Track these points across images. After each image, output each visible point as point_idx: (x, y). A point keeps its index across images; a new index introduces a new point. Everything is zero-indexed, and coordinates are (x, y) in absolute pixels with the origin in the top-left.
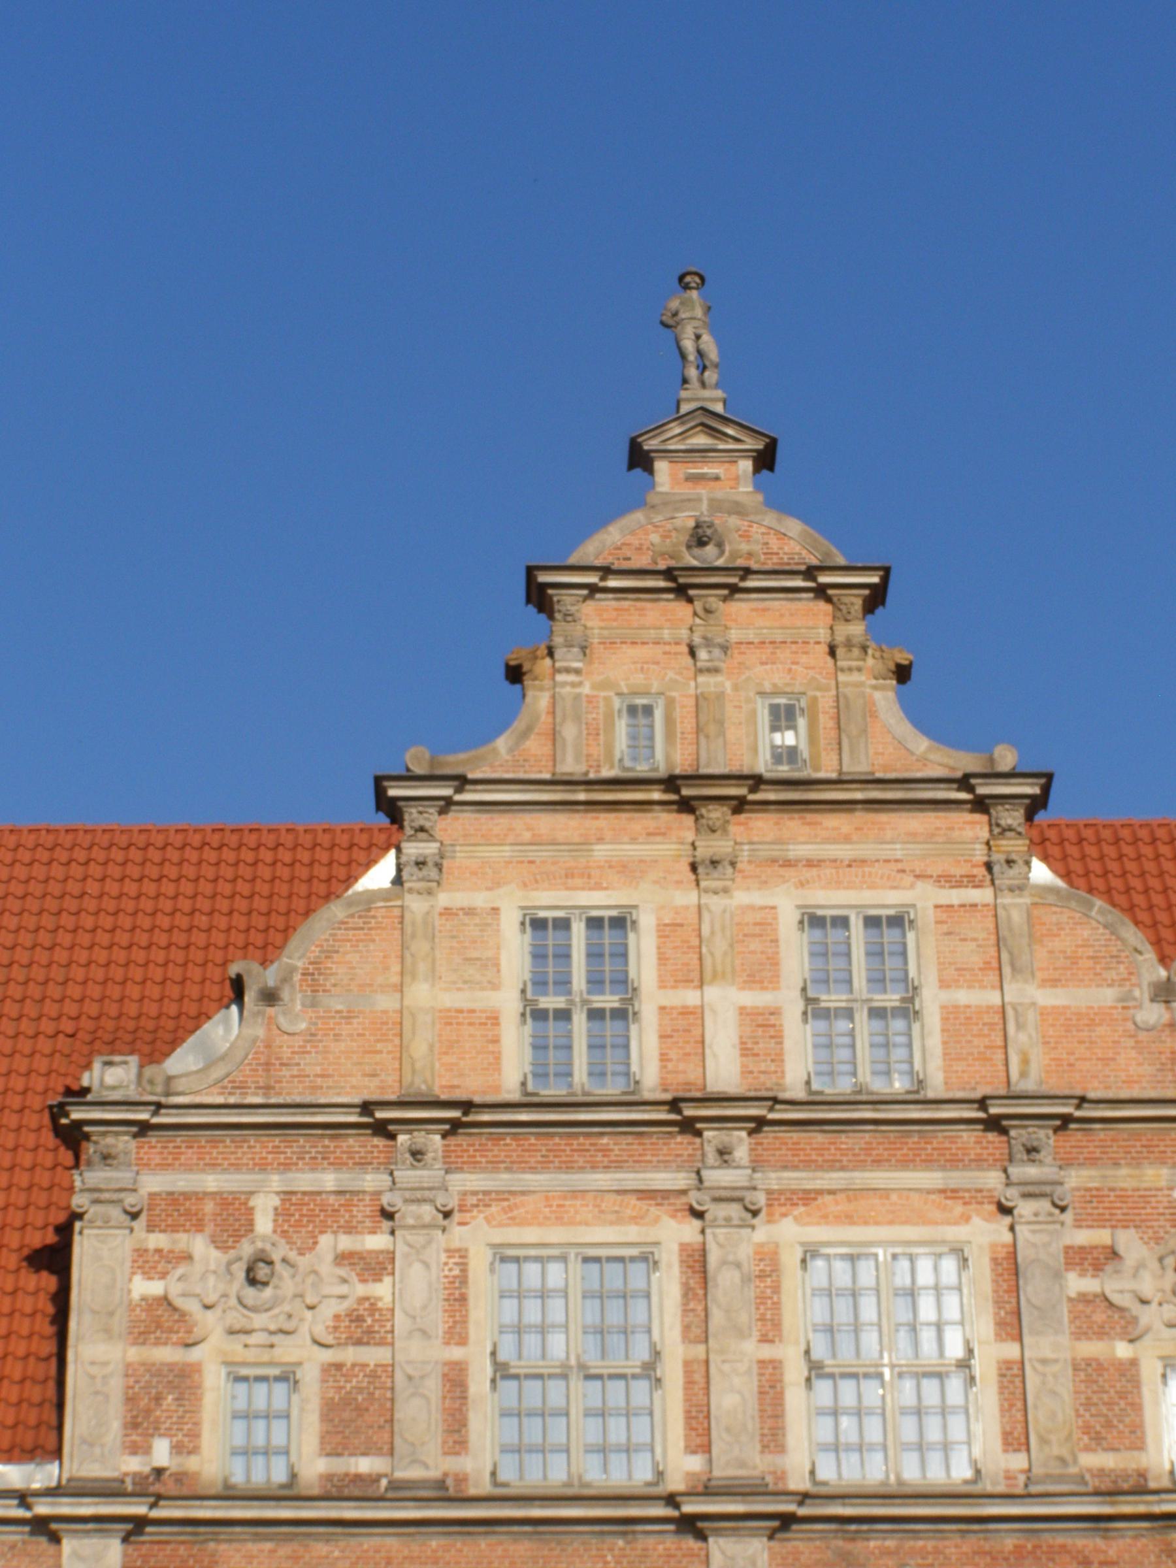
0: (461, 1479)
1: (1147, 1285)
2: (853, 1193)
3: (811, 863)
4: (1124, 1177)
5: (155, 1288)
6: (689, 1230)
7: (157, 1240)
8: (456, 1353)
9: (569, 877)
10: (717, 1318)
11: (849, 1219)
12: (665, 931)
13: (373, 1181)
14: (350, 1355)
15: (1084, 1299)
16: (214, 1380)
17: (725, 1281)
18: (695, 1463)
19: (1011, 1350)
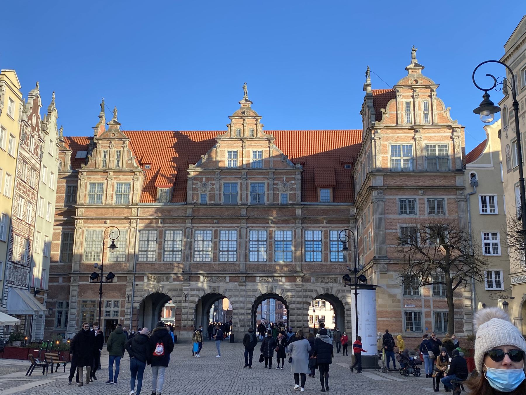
0: (221, 203)
1: (280, 187)
2: (255, 178)
3: (254, 146)
4: (279, 176)
5: (195, 186)
6: (241, 181)
7: (195, 182)
8: (220, 192)
9: (231, 147)
10: (243, 189)
11: (255, 180)
12: (240, 152)
13: (213, 176)
14: (211, 192)
15: (275, 187)
16: (199, 194)
17: (244, 186)
18: (240, 202)
19: (268, 192)
